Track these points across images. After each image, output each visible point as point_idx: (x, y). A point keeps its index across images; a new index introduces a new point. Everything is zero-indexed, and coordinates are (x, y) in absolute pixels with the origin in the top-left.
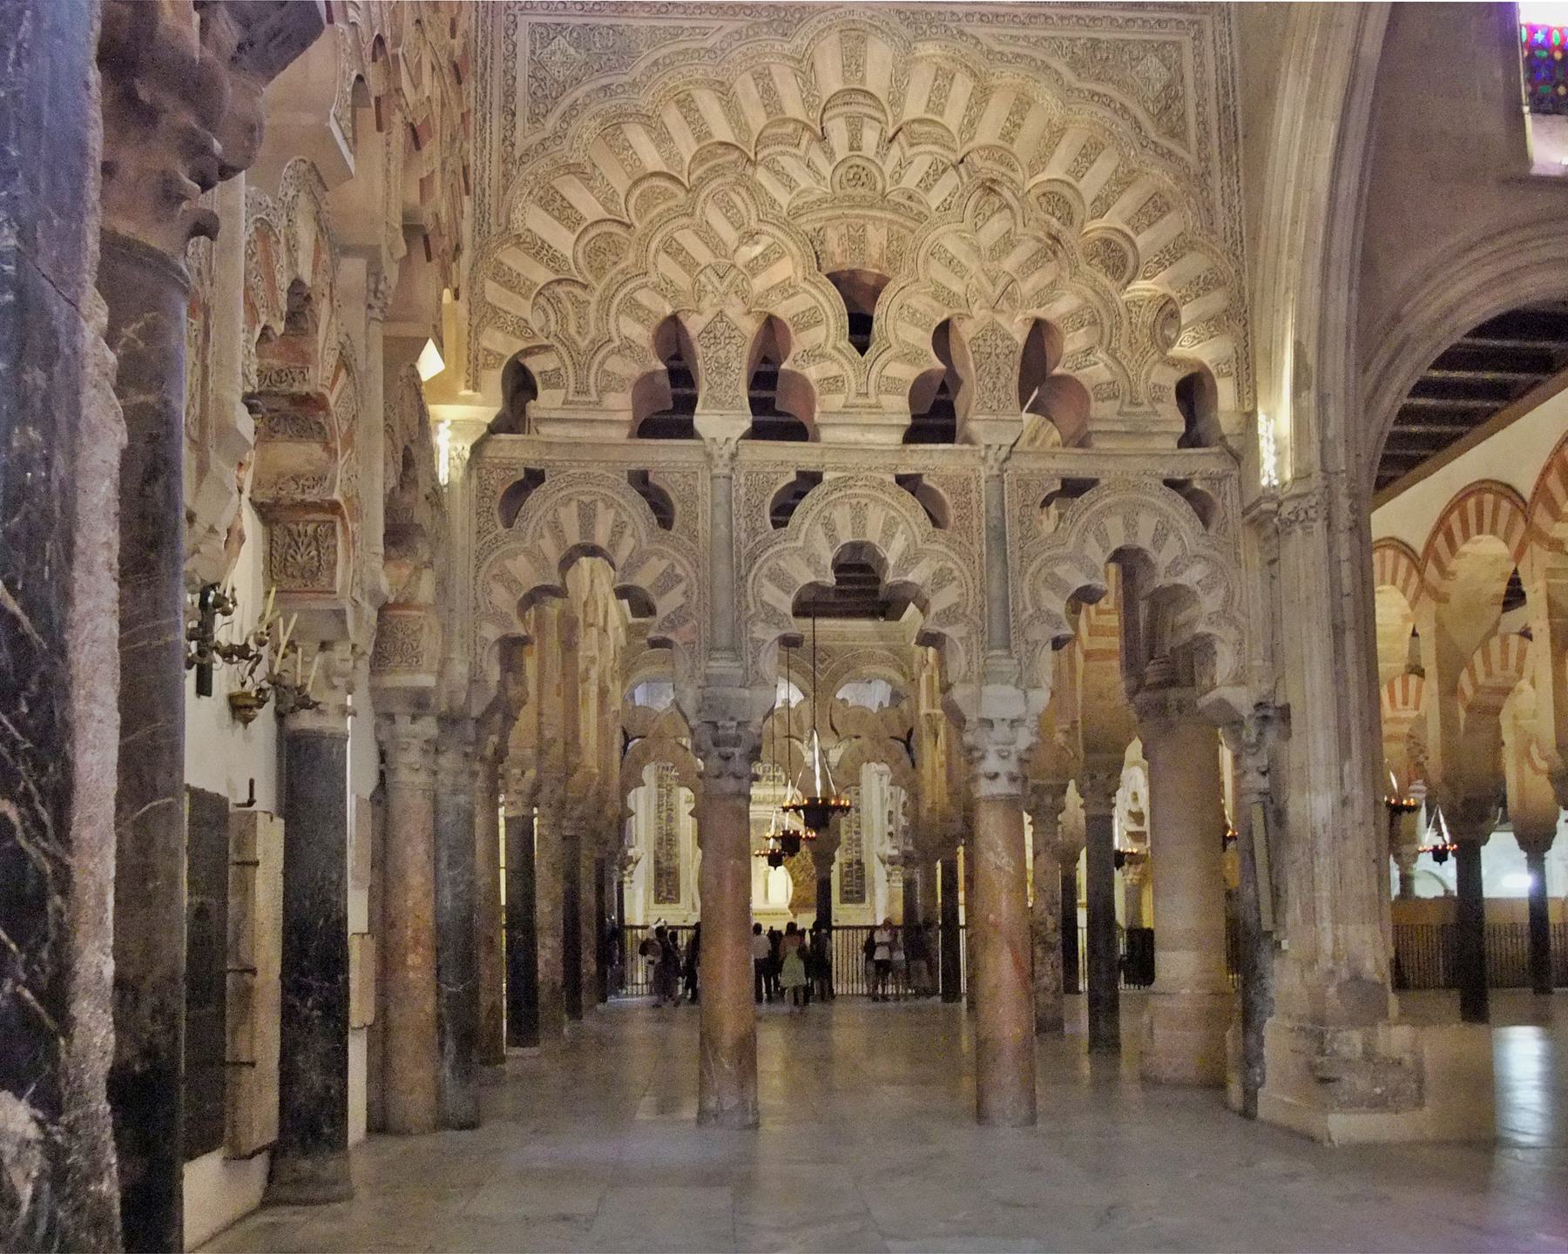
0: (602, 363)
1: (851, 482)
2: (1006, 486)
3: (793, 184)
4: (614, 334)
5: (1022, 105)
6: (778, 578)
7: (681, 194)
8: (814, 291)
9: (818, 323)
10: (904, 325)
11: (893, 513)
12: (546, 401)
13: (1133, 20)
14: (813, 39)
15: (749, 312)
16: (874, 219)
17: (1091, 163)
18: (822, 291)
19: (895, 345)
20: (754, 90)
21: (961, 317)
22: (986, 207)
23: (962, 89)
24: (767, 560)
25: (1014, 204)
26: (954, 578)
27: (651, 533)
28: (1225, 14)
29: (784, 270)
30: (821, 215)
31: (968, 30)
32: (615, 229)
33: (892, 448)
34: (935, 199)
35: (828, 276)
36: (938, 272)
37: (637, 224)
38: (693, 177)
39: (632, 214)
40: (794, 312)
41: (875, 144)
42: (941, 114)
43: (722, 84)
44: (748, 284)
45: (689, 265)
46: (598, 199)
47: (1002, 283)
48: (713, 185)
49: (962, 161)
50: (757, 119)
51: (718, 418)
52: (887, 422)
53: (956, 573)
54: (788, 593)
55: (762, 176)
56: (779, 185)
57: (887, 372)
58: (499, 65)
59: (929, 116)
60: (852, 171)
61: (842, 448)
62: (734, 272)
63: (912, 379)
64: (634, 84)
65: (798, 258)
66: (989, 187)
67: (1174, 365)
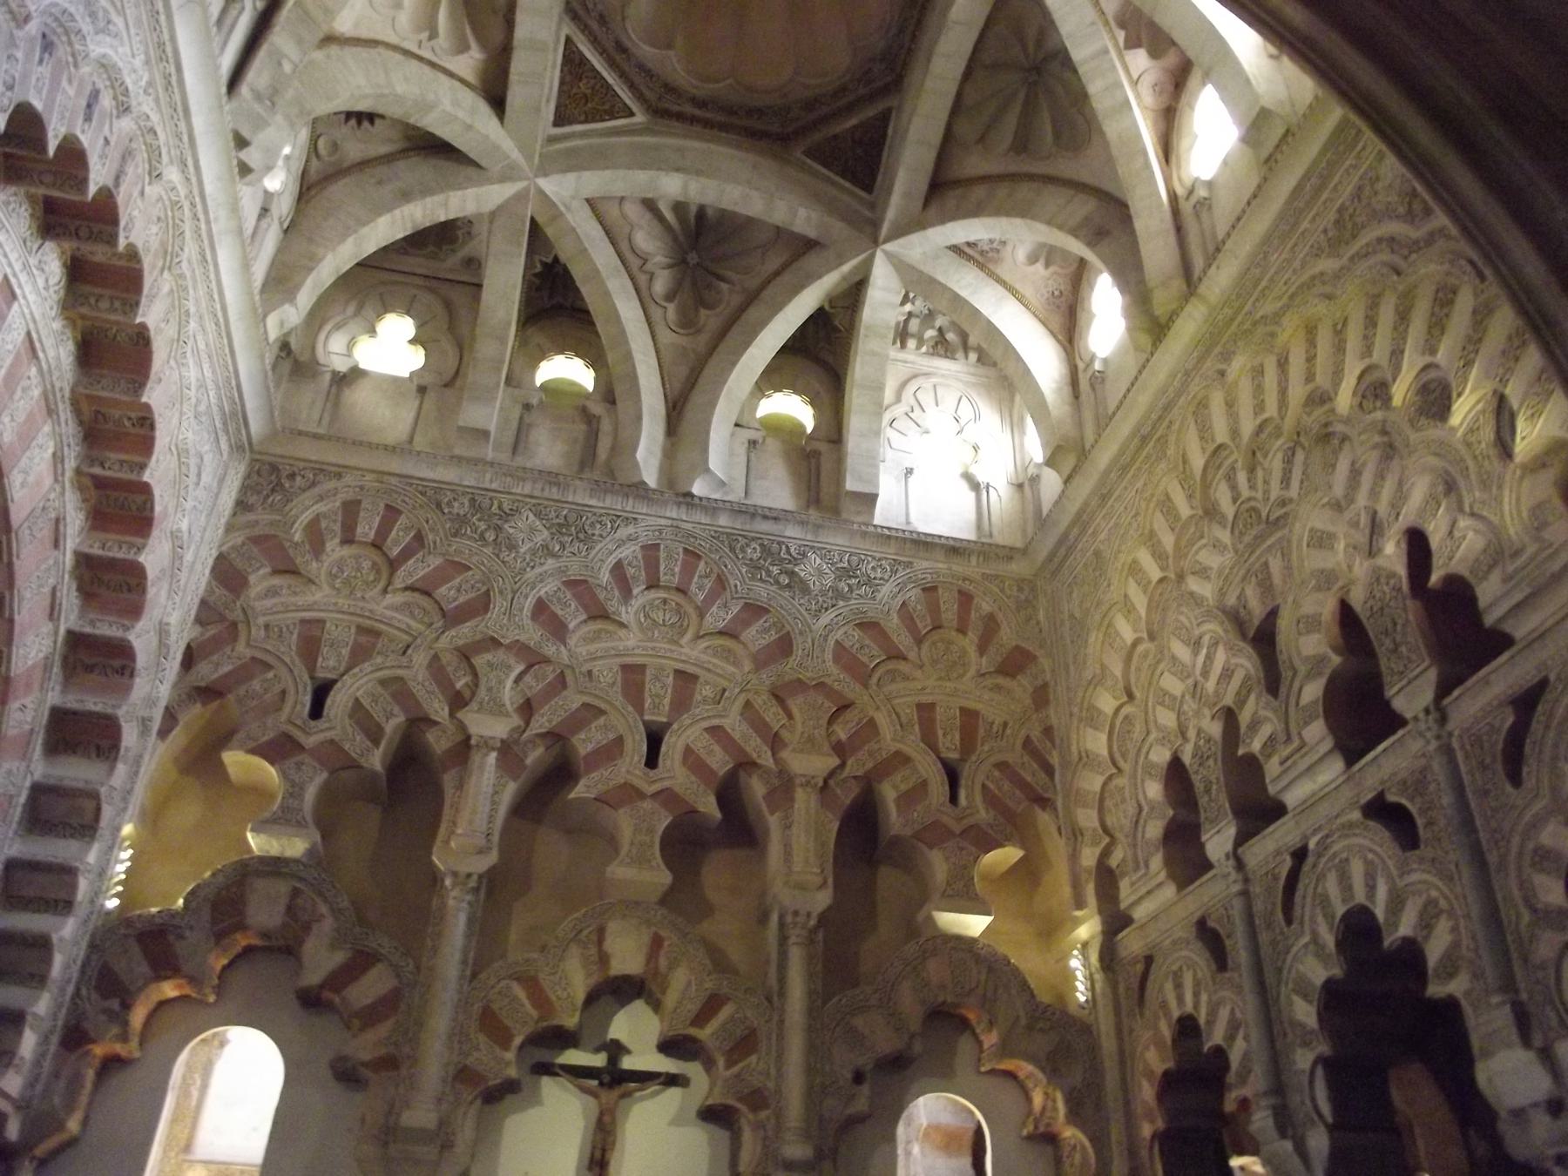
0: (1144, 832)
1: (1329, 840)
2: (1460, 756)
4: (1143, 802)
6: (1303, 990)
11: (1370, 856)
12: (1126, 892)
14: (1178, 440)
15: (1213, 718)
21: (1346, 589)
24: (1289, 972)
26: (1441, 911)
27: (1214, 983)
29: (1220, 657)
32: (1127, 709)
33: (1341, 779)
34: (1294, 492)
36: (1319, 560)
37: (1138, 694)
45: (1174, 703)
47: (1364, 520)
49: (1298, 434)
51: (1216, 838)
52: (1316, 757)
53: (1443, 904)
54: (1310, 1002)
55: (1194, 584)
59: (1258, 421)
61: (1309, 805)
63: (1320, 693)
66: (1325, 437)
67: (1544, 465)
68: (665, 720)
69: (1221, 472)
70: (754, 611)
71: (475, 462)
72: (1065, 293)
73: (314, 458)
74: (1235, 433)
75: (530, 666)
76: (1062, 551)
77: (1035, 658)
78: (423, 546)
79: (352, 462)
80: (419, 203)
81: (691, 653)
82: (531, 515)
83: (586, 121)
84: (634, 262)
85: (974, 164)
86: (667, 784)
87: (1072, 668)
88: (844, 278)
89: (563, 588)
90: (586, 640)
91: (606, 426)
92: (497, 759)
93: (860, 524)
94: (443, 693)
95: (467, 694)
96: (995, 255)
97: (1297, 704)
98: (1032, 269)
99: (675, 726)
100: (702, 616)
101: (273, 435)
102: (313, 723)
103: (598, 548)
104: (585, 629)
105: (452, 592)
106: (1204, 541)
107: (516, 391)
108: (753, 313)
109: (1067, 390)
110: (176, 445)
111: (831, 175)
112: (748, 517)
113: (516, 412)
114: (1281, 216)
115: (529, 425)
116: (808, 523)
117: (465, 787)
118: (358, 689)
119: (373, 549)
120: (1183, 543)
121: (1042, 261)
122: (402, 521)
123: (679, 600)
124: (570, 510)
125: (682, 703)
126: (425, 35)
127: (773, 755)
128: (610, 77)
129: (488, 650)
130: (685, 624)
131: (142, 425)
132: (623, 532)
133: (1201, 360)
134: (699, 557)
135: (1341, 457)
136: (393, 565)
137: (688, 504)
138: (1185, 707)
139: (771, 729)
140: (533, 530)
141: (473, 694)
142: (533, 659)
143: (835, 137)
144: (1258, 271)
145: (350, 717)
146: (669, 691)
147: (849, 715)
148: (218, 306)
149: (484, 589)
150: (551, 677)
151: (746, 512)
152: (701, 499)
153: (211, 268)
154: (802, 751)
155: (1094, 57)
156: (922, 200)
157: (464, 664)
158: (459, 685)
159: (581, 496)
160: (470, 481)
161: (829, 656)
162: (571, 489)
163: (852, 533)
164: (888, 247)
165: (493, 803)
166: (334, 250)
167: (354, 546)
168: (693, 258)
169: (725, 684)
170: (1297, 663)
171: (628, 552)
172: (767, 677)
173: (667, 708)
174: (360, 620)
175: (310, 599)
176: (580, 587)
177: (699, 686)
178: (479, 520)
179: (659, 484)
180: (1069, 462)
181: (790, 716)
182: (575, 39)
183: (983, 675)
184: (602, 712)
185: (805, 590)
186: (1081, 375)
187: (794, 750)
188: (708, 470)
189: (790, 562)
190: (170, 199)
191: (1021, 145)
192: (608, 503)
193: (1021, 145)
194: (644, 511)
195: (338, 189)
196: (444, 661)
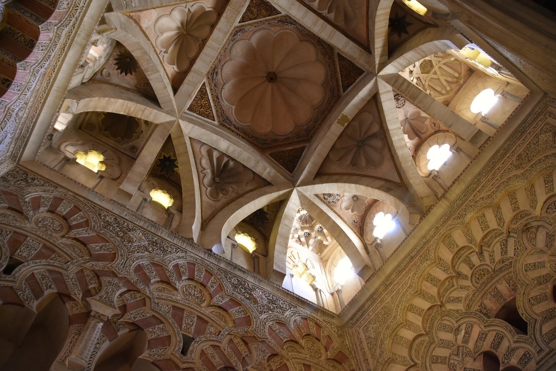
3: (460, 299)
5: (512, 196)
7: (426, 338)
8: (491, 328)
9: (502, 338)
10: (536, 307)
13: (526, 137)
14: (435, 252)
15: (475, 360)
16: (497, 281)
17: (552, 181)
18: (494, 325)
19: (538, 319)
20: (429, 284)
22: (532, 235)
23: (490, 216)
25: (540, 223)
28: (552, 100)
30: (477, 299)
31: (477, 199)
34: (511, 252)
35: (495, 318)
36: (533, 274)
38: (427, 330)
39: (416, 360)
40: (490, 344)
41: (478, 259)
42: (488, 227)
43: (417, 291)
44: (468, 348)
46: (400, 364)
48: (435, 325)
49: (509, 232)
50: (433, 291)
55: (449, 306)
56: (455, 304)
57: (544, 332)
58: (359, 348)
60: (477, 275)
62: (461, 348)
64: (395, 317)
65: (478, 322)
66: (526, 229)
68: (192, 336)
69: (461, 259)
70: (235, 302)
71: (122, 205)
72: (359, 222)
73: (47, 177)
74: (471, 240)
75: (129, 291)
76: (360, 313)
77: (348, 358)
78: (88, 226)
79: (64, 185)
80: (135, 104)
81: (207, 311)
82: (141, 234)
83: (198, 114)
84: (200, 169)
85: (334, 168)
86: (191, 365)
87: (370, 361)
88: (279, 197)
89: (150, 265)
90: (158, 290)
91: (177, 218)
92: (102, 327)
93: (277, 285)
94: (81, 287)
95: (93, 292)
96: (334, 204)
97: (541, 333)
98: (347, 211)
99: (197, 339)
100: (211, 297)
101: (32, 161)
102: (4, 275)
103: (168, 256)
104: (157, 285)
105: (97, 248)
106: (454, 288)
107: (142, 193)
108: (240, 200)
109: (364, 250)
110: (9, 108)
111: (278, 164)
112: (233, 267)
113: (141, 199)
114: (487, 165)
115: (144, 207)
116: (256, 278)
117: (82, 335)
118: (35, 270)
119: (62, 219)
120: (442, 291)
121: (351, 209)
122: (81, 213)
123: (201, 289)
124: (158, 238)
125: (199, 331)
126: (164, 50)
127: (243, 368)
128: (212, 104)
129: (109, 276)
130: (204, 299)
131: (3, 83)
132: (180, 254)
133: (444, 222)
134: (212, 275)
135: (538, 234)
136: (70, 228)
137: (209, 254)
138: (452, 361)
139: (242, 355)
140: (140, 239)
141: (97, 293)
142: (132, 289)
143: (283, 151)
144: (475, 186)
145: (26, 280)
146: (194, 324)
147: (276, 359)
148: (54, 76)
149: (113, 252)
150: (139, 299)
151: (232, 265)
152: (214, 254)
153: (64, 54)
154: (256, 369)
155: (395, 129)
156: (314, 176)
157: (96, 278)
158: (90, 287)
159: (164, 235)
160: (116, 211)
161: (267, 331)
162: (161, 231)
163: (274, 287)
164: (300, 189)
165: (96, 348)
166: (100, 97)
167: (53, 215)
168: (217, 180)
169: (221, 329)
170: (535, 317)
171: (181, 262)
172: (240, 331)
173: (193, 331)
174: (47, 243)
175: (23, 225)
176: (159, 267)
177: (208, 327)
178: (117, 227)
179: (197, 242)
180: (368, 274)
181: (250, 353)
182: (206, 85)
183: (328, 359)
184: (162, 323)
185: (256, 302)
186: (368, 246)
187: (252, 367)
188: (220, 242)
189: (249, 290)
190: (75, 3)
191: (354, 163)
192: (175, 242)
193: (354, 163)
194: (190, 250)
195: (105, 86)
196: (86, 274)
